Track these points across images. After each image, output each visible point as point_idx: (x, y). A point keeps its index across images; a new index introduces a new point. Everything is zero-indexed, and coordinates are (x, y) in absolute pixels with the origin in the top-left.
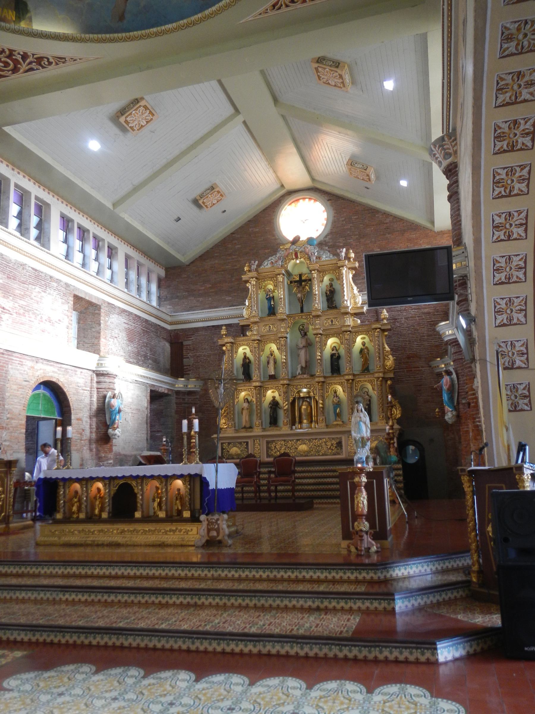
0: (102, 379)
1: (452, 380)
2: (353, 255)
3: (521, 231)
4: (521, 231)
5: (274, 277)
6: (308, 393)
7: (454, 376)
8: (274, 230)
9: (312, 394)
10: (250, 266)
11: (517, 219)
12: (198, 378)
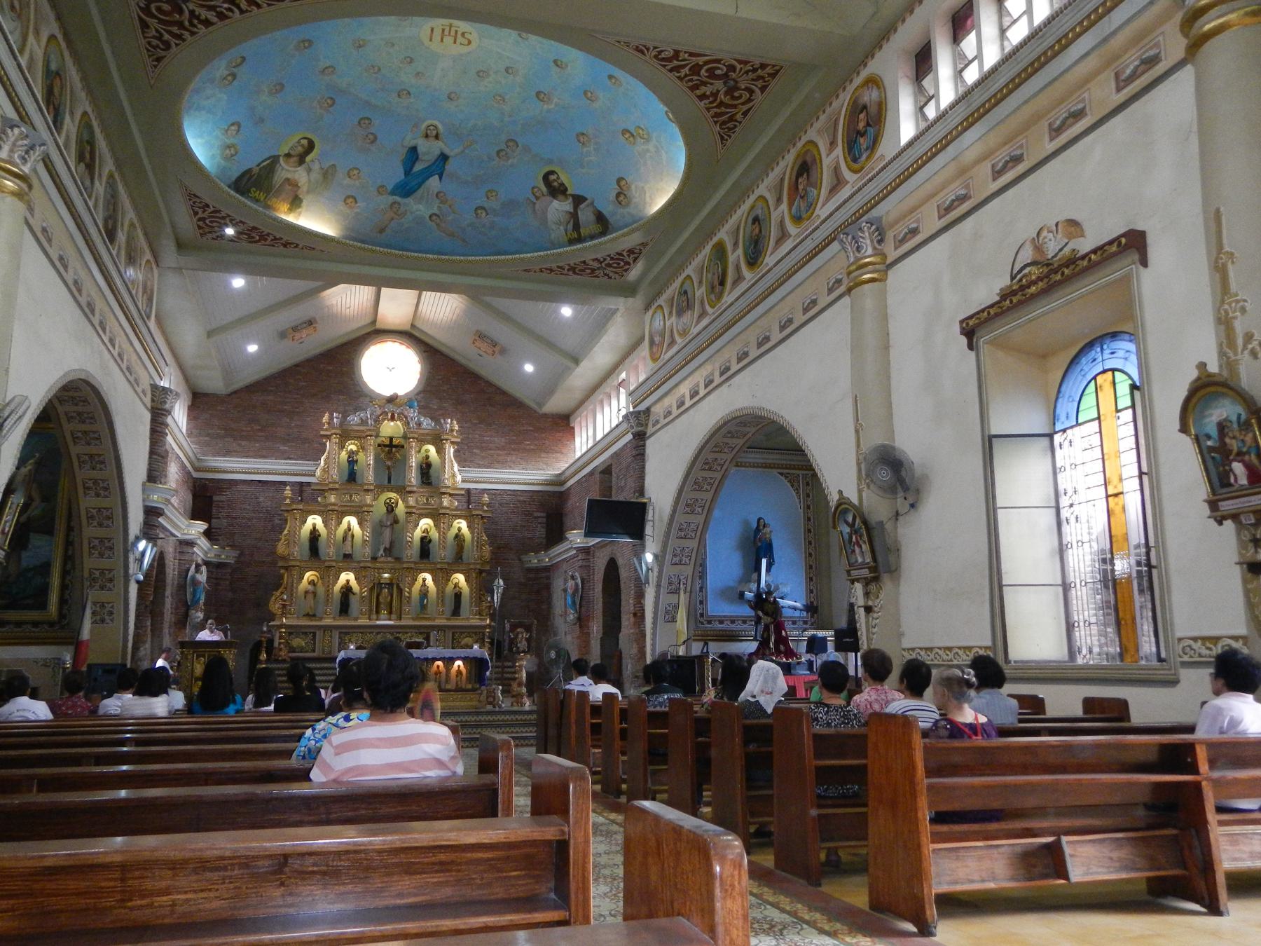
0: (186, 549)
1: (577, 585)
2: (457, 428)
3: (700, 510)
4: (700, 510)
5: (360, 437)
6: (391, 579)
7: (579, 581)
8: (354, 374)
9: (394, 581)
10: (331, 418)
11: (700, 503)
12: (233, 546)
